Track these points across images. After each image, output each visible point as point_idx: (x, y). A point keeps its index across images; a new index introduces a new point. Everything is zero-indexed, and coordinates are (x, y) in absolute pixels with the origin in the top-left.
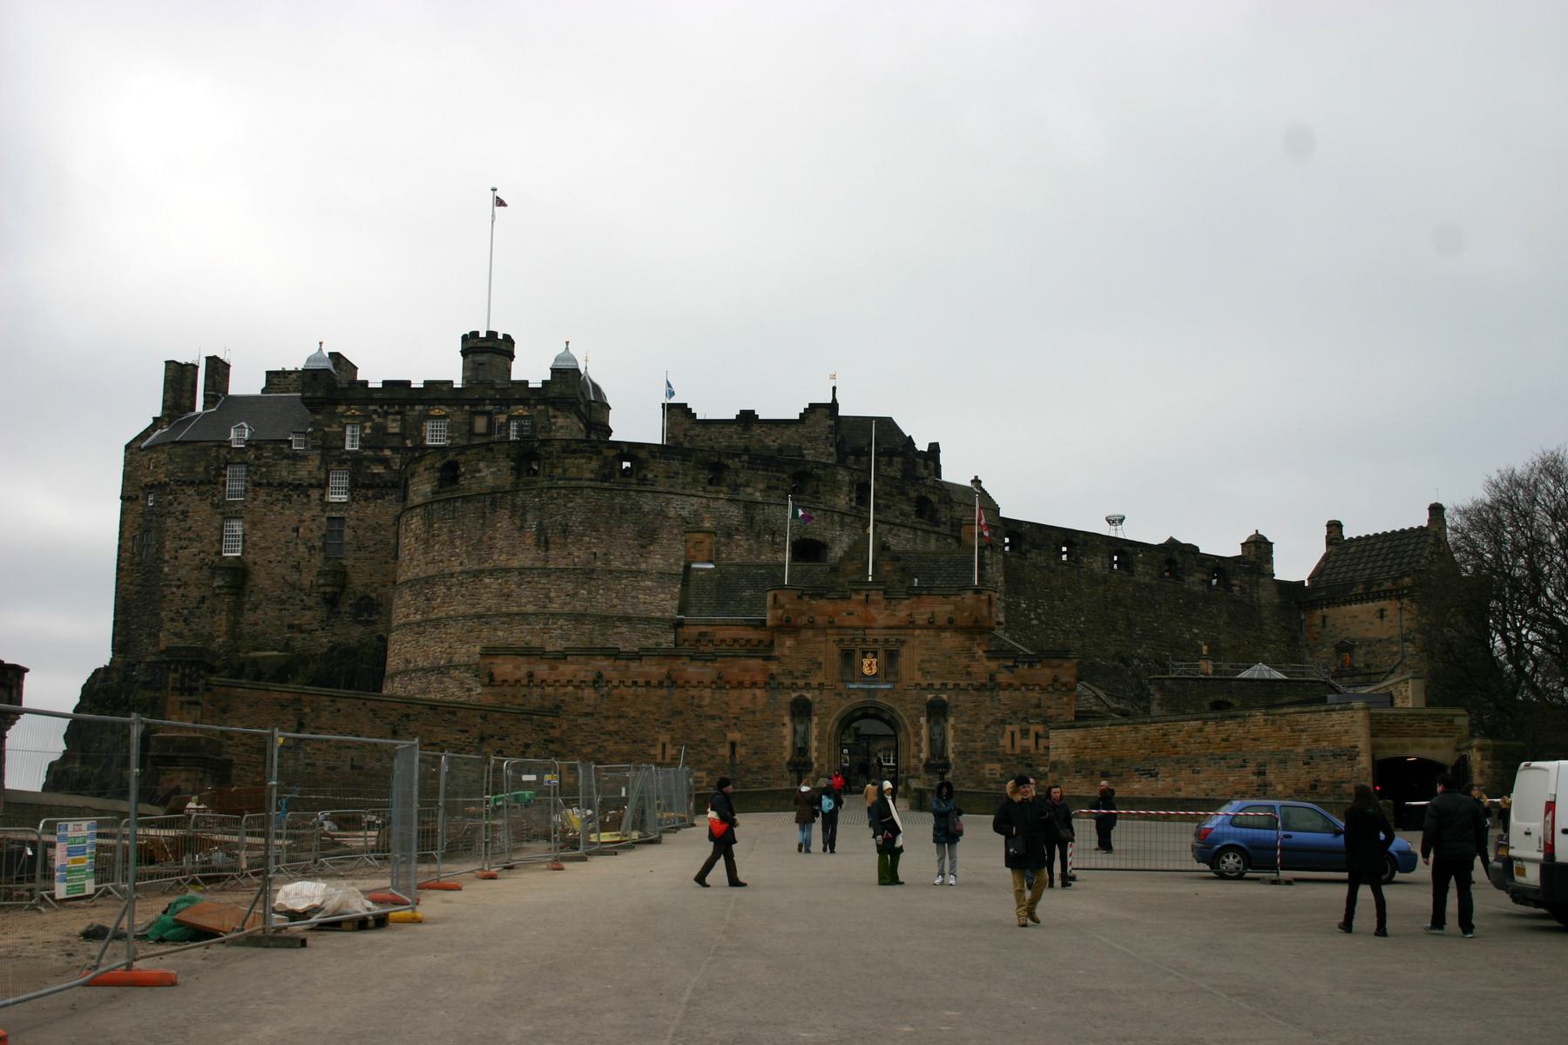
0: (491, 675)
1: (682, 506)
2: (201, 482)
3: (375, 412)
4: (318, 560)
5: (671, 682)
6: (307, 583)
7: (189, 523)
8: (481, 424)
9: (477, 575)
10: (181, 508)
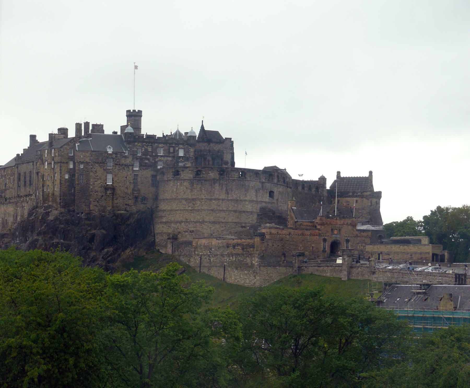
0: (271, 233)
1: (252, 184)
2: (101, 163)
3: (145, 145)
4: (132, 186)
5: (303, 234)
6: (129, 193)
7: (97, 174)
8: (172, 150)
9: (211, 200)
10: (95, 170)
